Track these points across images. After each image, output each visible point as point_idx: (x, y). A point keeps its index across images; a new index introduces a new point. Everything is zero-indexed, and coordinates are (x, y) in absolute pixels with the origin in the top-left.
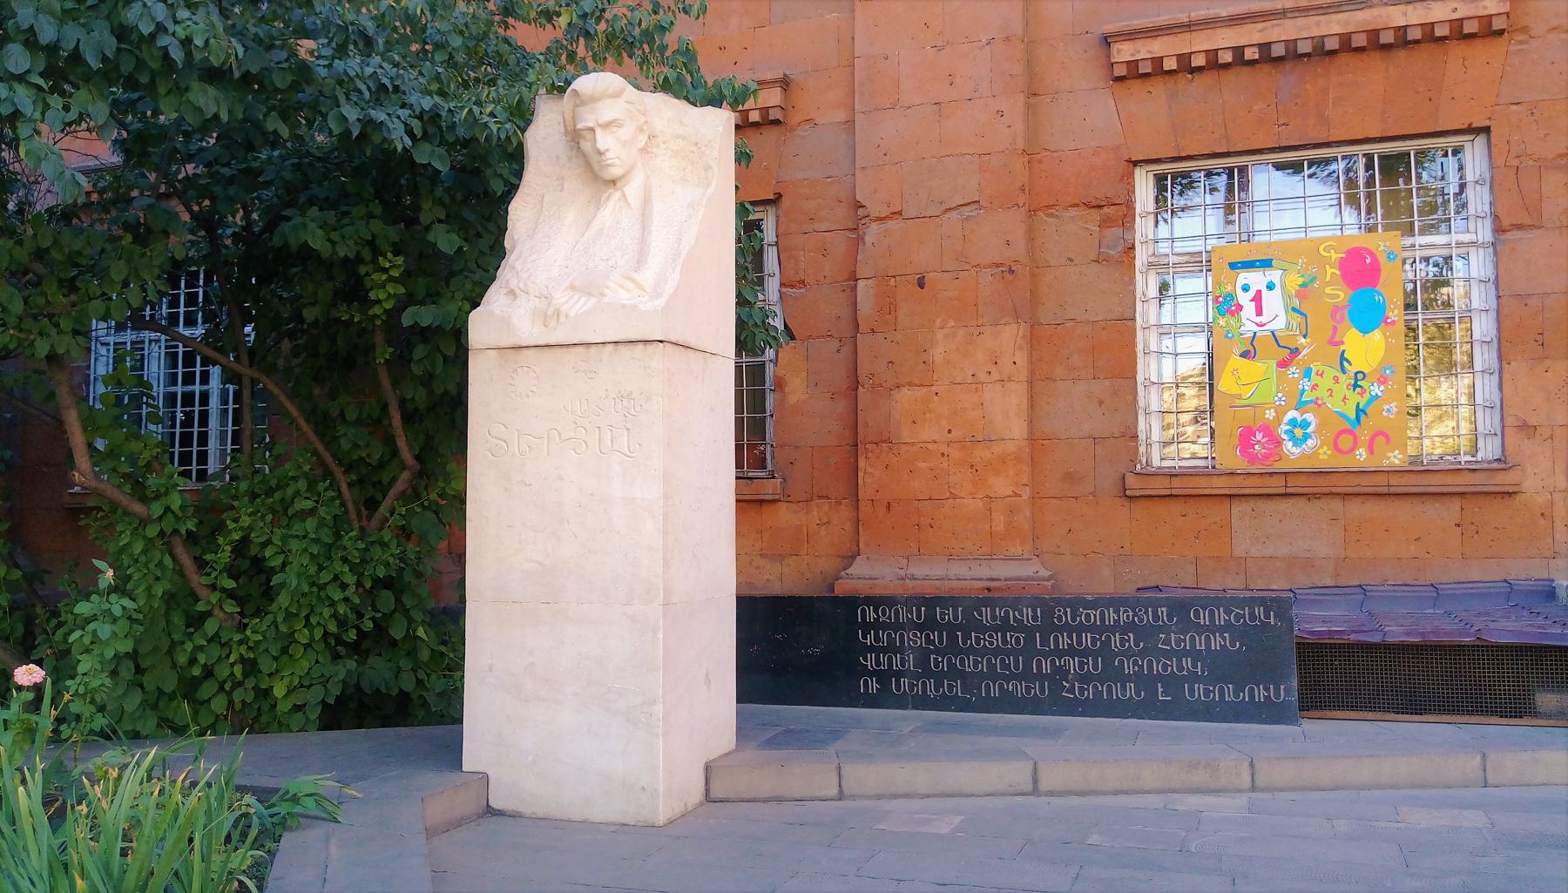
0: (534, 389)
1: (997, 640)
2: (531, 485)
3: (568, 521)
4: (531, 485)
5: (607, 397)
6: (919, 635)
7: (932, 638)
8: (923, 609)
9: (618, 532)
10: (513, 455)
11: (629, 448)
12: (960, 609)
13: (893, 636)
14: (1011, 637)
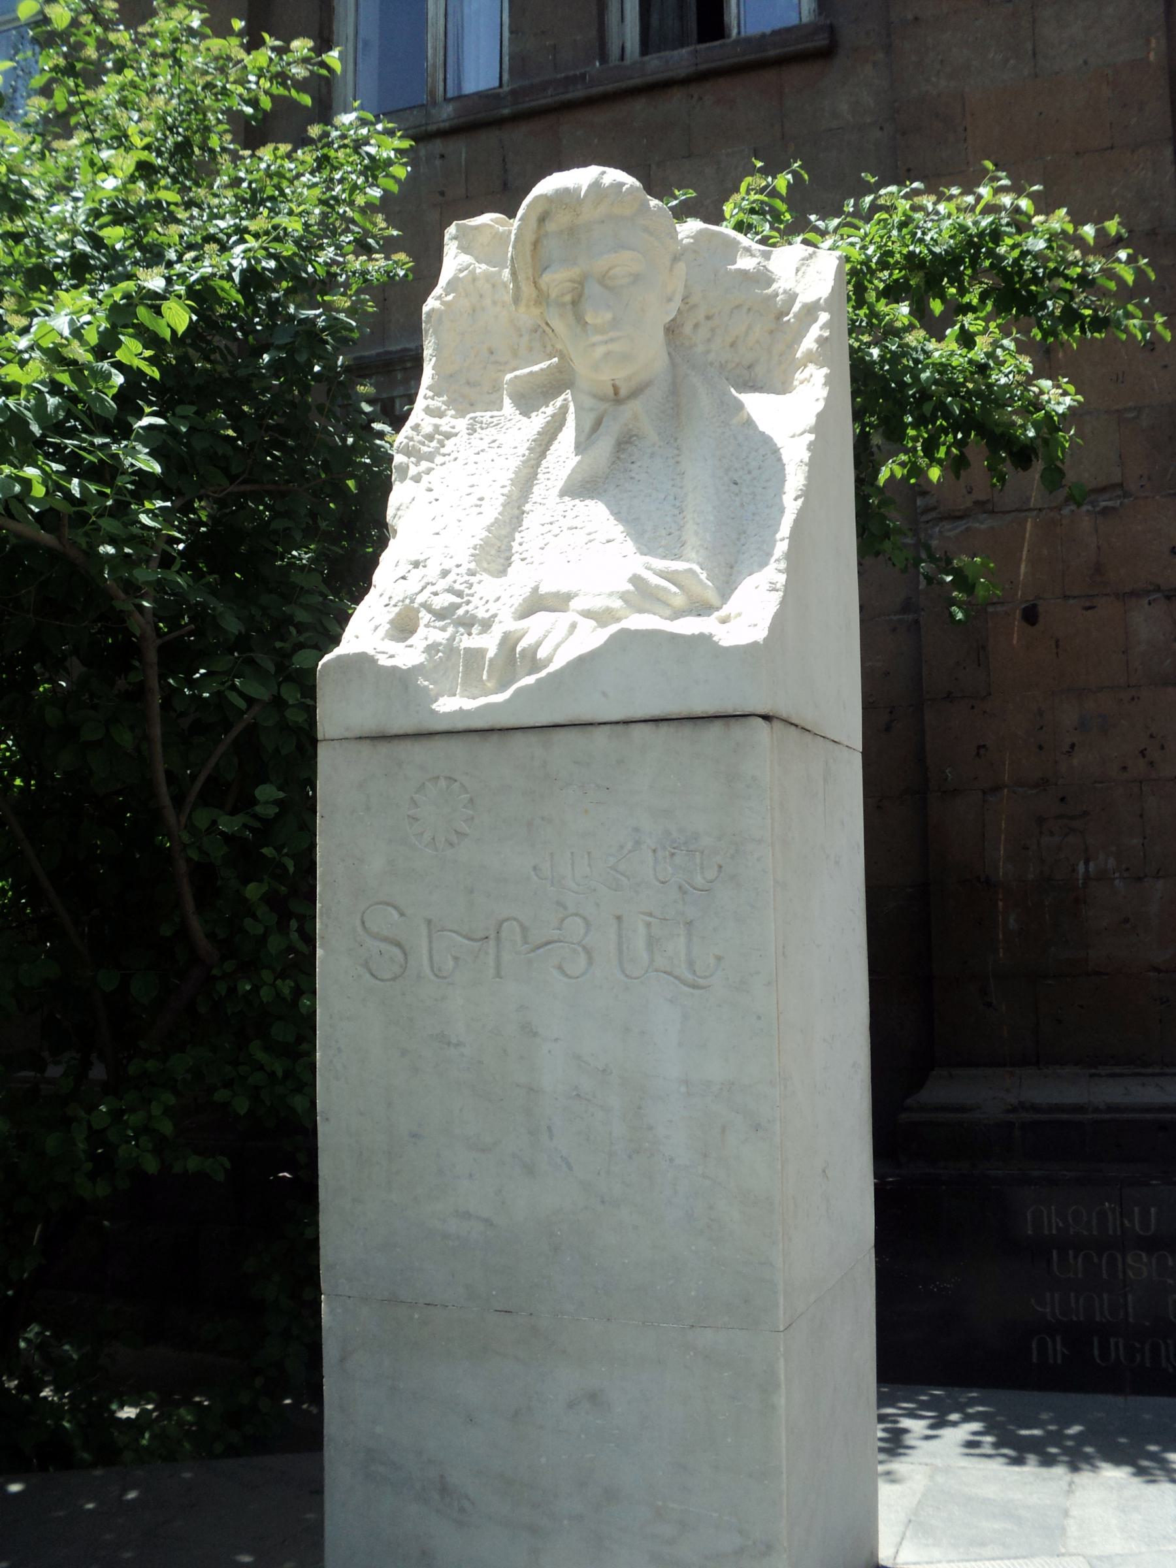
0: (464, 828)
2: (459, 1044)
3: (549, 1129)
4: (458, 1045)
5: (638, 843)
6: (1145, 1260)
8: (1153, 1210)
9: (671, 1160)
11: (691, 964)
13: (1096, 1260)
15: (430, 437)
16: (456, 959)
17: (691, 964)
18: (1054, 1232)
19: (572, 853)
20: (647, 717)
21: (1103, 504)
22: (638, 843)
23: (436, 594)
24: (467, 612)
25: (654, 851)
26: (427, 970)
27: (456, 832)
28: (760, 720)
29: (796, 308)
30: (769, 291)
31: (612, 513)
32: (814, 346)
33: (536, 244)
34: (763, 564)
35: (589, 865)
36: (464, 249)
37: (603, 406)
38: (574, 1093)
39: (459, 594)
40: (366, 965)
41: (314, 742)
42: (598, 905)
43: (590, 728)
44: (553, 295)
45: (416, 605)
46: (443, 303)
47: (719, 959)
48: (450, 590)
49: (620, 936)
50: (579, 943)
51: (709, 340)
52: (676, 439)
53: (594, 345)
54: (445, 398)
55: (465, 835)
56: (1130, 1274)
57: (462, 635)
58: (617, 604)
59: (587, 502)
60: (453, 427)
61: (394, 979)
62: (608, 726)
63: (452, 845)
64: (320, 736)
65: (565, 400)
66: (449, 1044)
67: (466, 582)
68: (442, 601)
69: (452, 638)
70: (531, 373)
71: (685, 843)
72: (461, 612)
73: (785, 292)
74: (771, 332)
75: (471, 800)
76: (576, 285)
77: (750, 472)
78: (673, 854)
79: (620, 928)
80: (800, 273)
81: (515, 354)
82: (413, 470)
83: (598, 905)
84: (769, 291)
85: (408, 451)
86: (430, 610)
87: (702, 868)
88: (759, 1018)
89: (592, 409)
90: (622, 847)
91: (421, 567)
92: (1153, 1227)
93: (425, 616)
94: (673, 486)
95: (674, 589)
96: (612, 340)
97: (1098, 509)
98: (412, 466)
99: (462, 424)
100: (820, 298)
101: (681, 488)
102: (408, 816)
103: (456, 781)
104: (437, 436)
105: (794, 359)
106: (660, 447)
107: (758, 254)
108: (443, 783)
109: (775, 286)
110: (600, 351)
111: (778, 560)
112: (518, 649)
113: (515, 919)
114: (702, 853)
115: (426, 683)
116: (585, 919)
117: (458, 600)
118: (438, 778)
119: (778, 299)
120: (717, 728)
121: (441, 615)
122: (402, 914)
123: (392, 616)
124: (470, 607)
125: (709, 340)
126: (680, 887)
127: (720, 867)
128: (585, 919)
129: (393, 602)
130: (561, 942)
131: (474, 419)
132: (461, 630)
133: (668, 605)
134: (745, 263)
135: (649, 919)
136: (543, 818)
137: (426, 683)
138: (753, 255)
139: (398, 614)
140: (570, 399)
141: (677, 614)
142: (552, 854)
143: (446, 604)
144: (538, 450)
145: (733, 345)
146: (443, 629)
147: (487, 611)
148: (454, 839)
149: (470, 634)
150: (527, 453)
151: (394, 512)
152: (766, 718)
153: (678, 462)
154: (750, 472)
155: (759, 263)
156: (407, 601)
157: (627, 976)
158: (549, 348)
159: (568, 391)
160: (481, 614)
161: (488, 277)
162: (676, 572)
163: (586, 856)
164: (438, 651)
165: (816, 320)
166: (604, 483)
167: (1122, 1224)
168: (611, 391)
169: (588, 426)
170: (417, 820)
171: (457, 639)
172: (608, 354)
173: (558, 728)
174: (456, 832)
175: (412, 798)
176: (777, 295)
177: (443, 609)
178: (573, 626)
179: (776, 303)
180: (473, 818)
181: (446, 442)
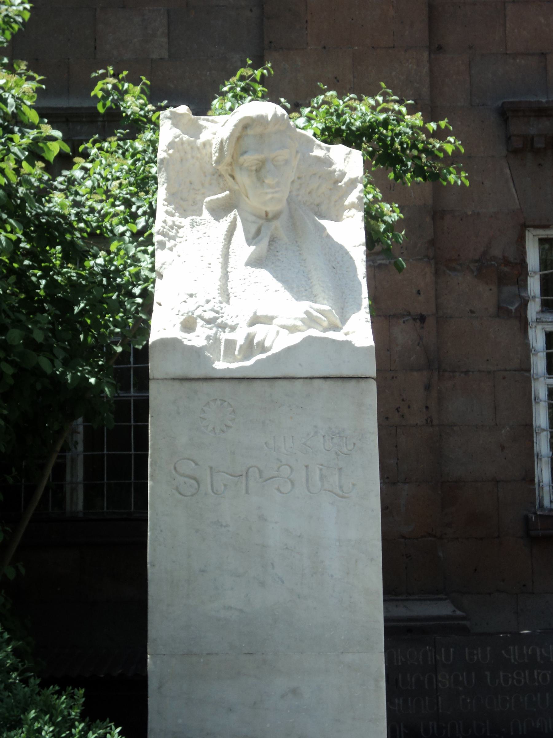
0: (230, 423)
1: (525, 678)
2: (226, 526)
3: (272, 564)
4: (226, 526)
5: (316, 433)
6: (447, 677)
7: (461, 679)
8: (452, 650)
10: (206, 494)
11: (341, 487)
12: (488, 649)
14: (538, 674)
15: (172, 227)
16: (225, 486)
17: (341, 487)
18: (400, 664)
19: (284, 437)
20: (321, 376)
21: (379, 262)
22: (316, 433)
23: (205, 311)
24: (222, 321)
25: (324, 436)
27: (226, 426)
28: (373, 380)
29: (346, 180)
30: (331, 169)
31: (274, 277)
32: (356, 201)
33: (239, 138)
34: (359, 309)
35: (293, 442)
36: (175, 125)
37: (261, 222)
38: (285, 547)
39: (217, 312)
40: (177, 489)
42: (297, 460)
43: (294, 380)
44: (246, 165)
45: (195, 316)
46: (168, 154)
47: (354, 485)
48: (213, 310)
49: (307, 475)
50: (288, 478)
51: (299, 190)
52: (297, 242)
53: (267, 193)
54: (173, 206)
55: (231, 427)
56: (440, 685)
57: (221, 332)
58: (299, 323)
59: (259, 270)
60: (181, 223)
61: (192, 495)
62: (302, 380)
63: (223, 431)
64: (151, 376)
65: (235, 214)
66: (221, 526)
67: (220, 307)
68: (209, 315)
69: (216, 334)
70: (218, 199)
71: (338, 433)
72: (219, 321)
73: (340, 171)
74: (330, 189)
75: (234, 411)
76: (259, 162)
77: (338, 263)
78: (332, 438)
80: (346, 161)
81: (203, 185)
82: (168, 245)
83: (297, 460)
84: (331, 169)
85: (164, 234)
86: (202, 318)
87: (346, 445)
88: (373, 511)
89: (254, 222)
90: (308, 434)
91: (194, 297)
92: (451, 658)
93: (200, 322)
94: (301, 266)
95: (324, 318)
96: (276, 192)
97: (376, 264)
98: (167, 242)
99: (186, 222)
100: (358, 177)
101: (305, 267)
102: (200, 417)
103: (225, 401)
104: (174, 227)
105: (343, 205)
106: (289, 245)
107: (325, 149)
108: (219, 402)
109: (334, 167)
110: (269, 196)
111: (365, 308)
112: (255, 341)
113: (255, 466)
114: (346, 438)
115: (209, 354)
116: (290, 467)
117: (217, 315)
118: (216, 400)
119: (336, 173)
120: (353, 383)
121: (209, 322)
122: (196, 464)
123: (181, 320)
124: (223, 319)
125: (299, 190)
126: (336, 453)
127: (354, 444)
128: (290, 467)
129: (181, 313)
130: (278, 477)
131: (192, 220)
132: (220, 330)
133: (321, 325)
134: (318, 152)
135: (321, 467)
136: (270, 420)
137: (209, 354)
138: (322, 149)
139: (184, 320)
140: (237, 214)
141: (325, 330)
142: (274, 437)
143: (211, 317)
144: (227, 240)
145: (309, 193)
146: (211, 329)
147: (233, 321)
148: (225, 429)
149: (224, 332)
150: (224, 241)
151: (160, 265)
153: (300, 254)
154: (338, 263)
155: (326, 154)
156: (190, 314)
157: (311, 493)
158: (222, 185)
159: (235, 210)
160: (230, 323)
161: (189, 143)
162: (324, 310)
163: (291, 438)
164: (210, 339)
165: (356, 187)
166: (265, 261)
167: (435, 658)
168: (264, 214)
169: (253, 229)
170: (205, 419)
171: (218, 334)
172: (272, 198)
173: (277, 379)
174: (226, 426)
175: (202, 409)
176: (335, 171)
177: (210, 319)
178: (278, 332)
179: (334, 175)
180: (234, 419)
181: (179, 231)
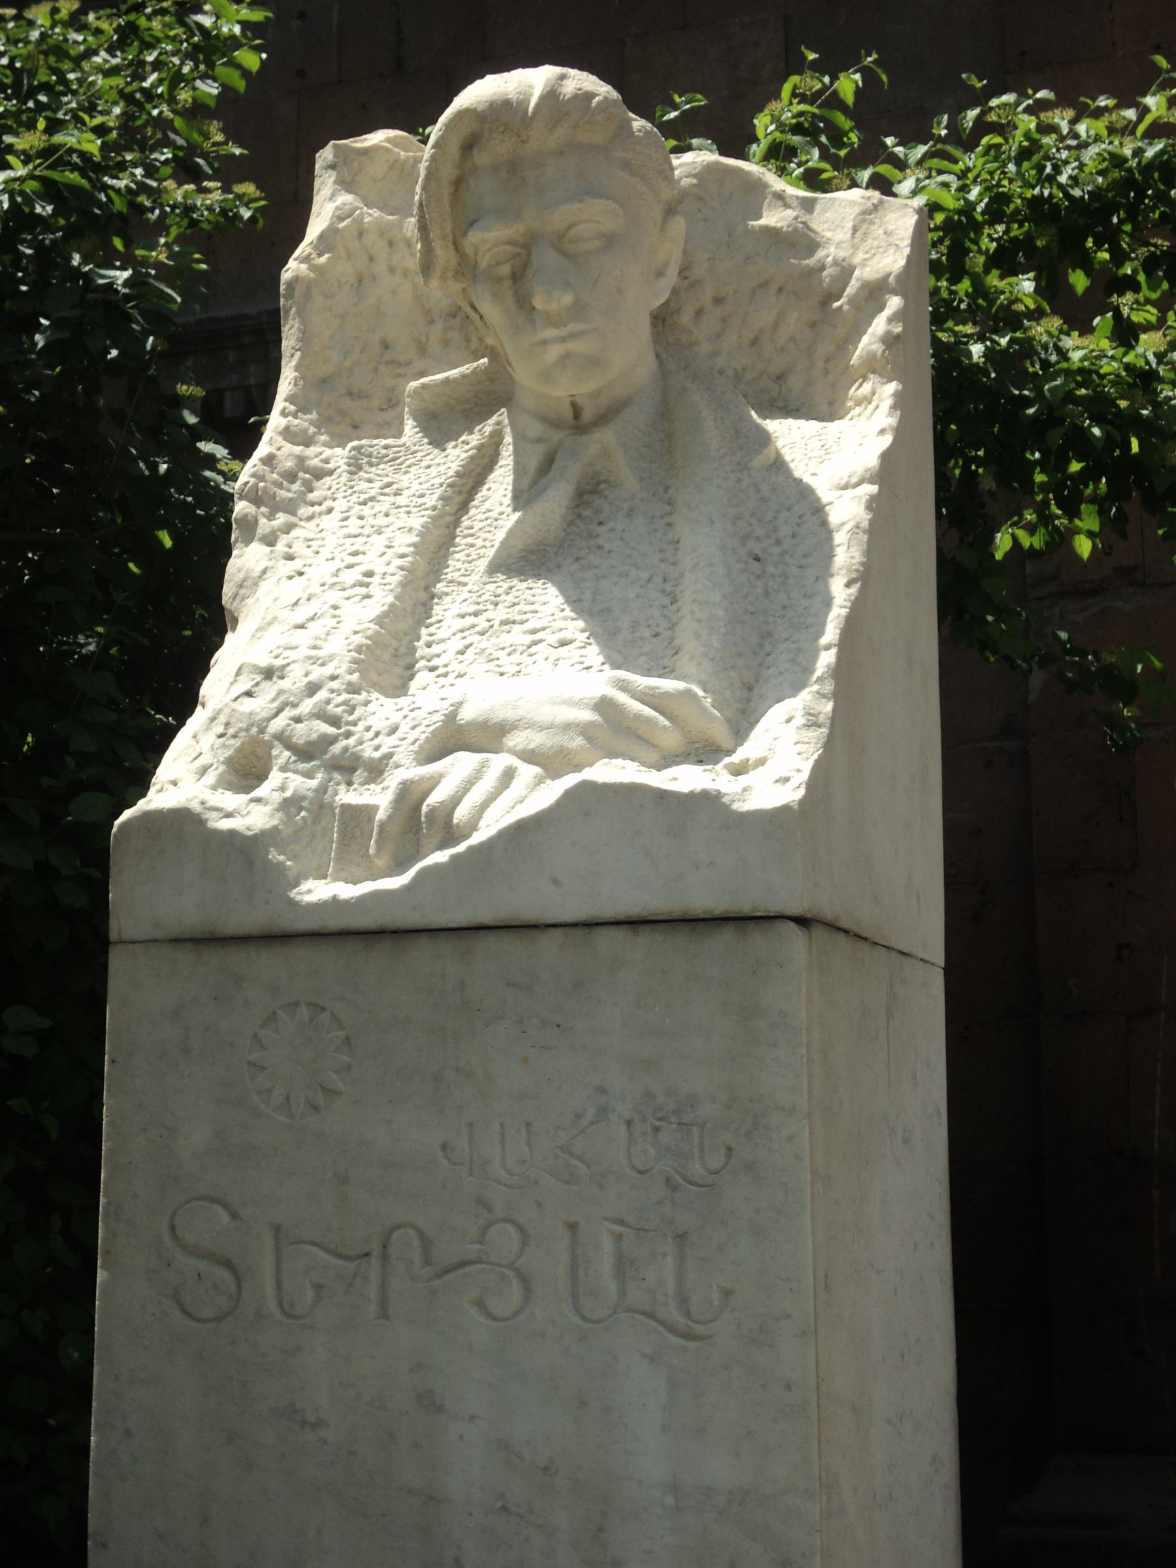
0: (337, 1082)
2: (319, 1424)
5: (603, 1111)
11: (683, 1300)
15: (291, 477)
16: (318, 1287)
17: (683, 1300)
19: (502, 1125)
22: (603, 1111)
23: (298, 720)
24: (346, 749)
25: (629, 1123)
26: (271, 1306)
27: (324, 1090)
28: (792, 924)
29: (850, 290)
30: (811, 262)
31: (569, 600)
32: (878, 348)
33: (458, 183)
34: (797, 687)
35: (529, 1144)
36: (345, 185)
37: (555, 436)
38: (499, 1504)
39: (335, 721)
40: (176, 1296)
41: (104, 943)
42: (539, 1205)
43: (533, 932)
44: (483, 264)
45: (267, 737)
46: (313, 268)
47: (727, 1293)
48: (320, 714)
49: (574, 1257)
50: (511, 1266)
51: (718, 336)
52: (667, 489)
53: (544, 343)
54: (314, 416)
55: (338, 1093)
57: (338, 784)
58: (578, 742)
59: (530, 583)
60: (327, 461)
61: (219, 1319)
62: (558, 933)
63: (316, 1108)
64: (113, 936)
65: (498, 423)
66: (303, 1422)
67: (344, 703)
68: (305, 732)
69: (322, 790)
70: (447, 381)
71: (676, 1112)
72: (337, 748)
73: (835, 263)
74: (813, 325)
75: (347, 1040)
76: (518, 250)
77: (778, 542)
78: (657, 1129)
79: (574, 1243)
80: (858, 234)
81: (422, 349)
82: (264, 526)
83: (539, 1205)
84: (811, 262)
85: (256, 499)
86: (289, 746)
87: (702, 1151)
88: (788, 1388)
89: (539, 440)
90: (578, 1116)
91: (275, 679)
93: (282, 755)
94: (662, 560)
95: (662, 719)
96: (573, 336)
98: (263, 521)
99: (339, 456)
100: (889, 275)
101: (675, 564)
102: (249, 1063)
103: (323, 1009)
104: (301, 474)
105: (847, 367)
106: (642, 500)
107: (795, 203)
108: (304, 1012)
109: (821, 253)
110: (554, 352)
111: (820, 680)
112: (424, 809)
114: (702, 1128)
115: (281, 858)
116: (520, 1228)
117: (331, 730)
118: (297, 1004)
119: (825, 273)
120: (726, 935)
121: (307, 752)
122: (234, 1216)
123: (228, 753)
124: (351, 741)
125: (718, 336)
126: (668, 1181)
127: (730, 1149)
128: (520, 1228)
129: (231, 731)
130: (480, 1262)
131: (358, 449)
132: (337, 776)
133: (654, 746)
134: (774, 218)
136: (457, 1070)
137: (281, 858)
138: (787, 206)
139: (240, 750)
140: (506, 421)
141: (666, 761)
142: (470, 1125)
143: (314, 736)
144: (458, 499)
145: (754, 343)
146: (309, 775)
147: (377, 748)
148: (320, 1099)
149: (349, 783)
150: (440, 504)
151: (234, 590)
152: (802, 921)
153: (669, 525)
154: (778, 542)
155: (796, 218)
156: (255, 730)
157: (583, 1317)
158: (475, 343)
159: (503, 410)
160: (368, 752)
161: (383, 231)
162: (667, 695)
163: (524, 1131)
164: (301, 809)
165: (881, 308)
166: (556, 554)
168: (568, 414)
169: (533, 463)
170: (263, 1069)
171: (330, 791)
172: (566, 356)
173: (481, 932)
174: (324, 1090)
175: (256, 1035)
176: (823, 268)
177: (311, 744)
178: (508, 776)
179: (821, 281)
180: (349, 1067)
181: (316, 484)
